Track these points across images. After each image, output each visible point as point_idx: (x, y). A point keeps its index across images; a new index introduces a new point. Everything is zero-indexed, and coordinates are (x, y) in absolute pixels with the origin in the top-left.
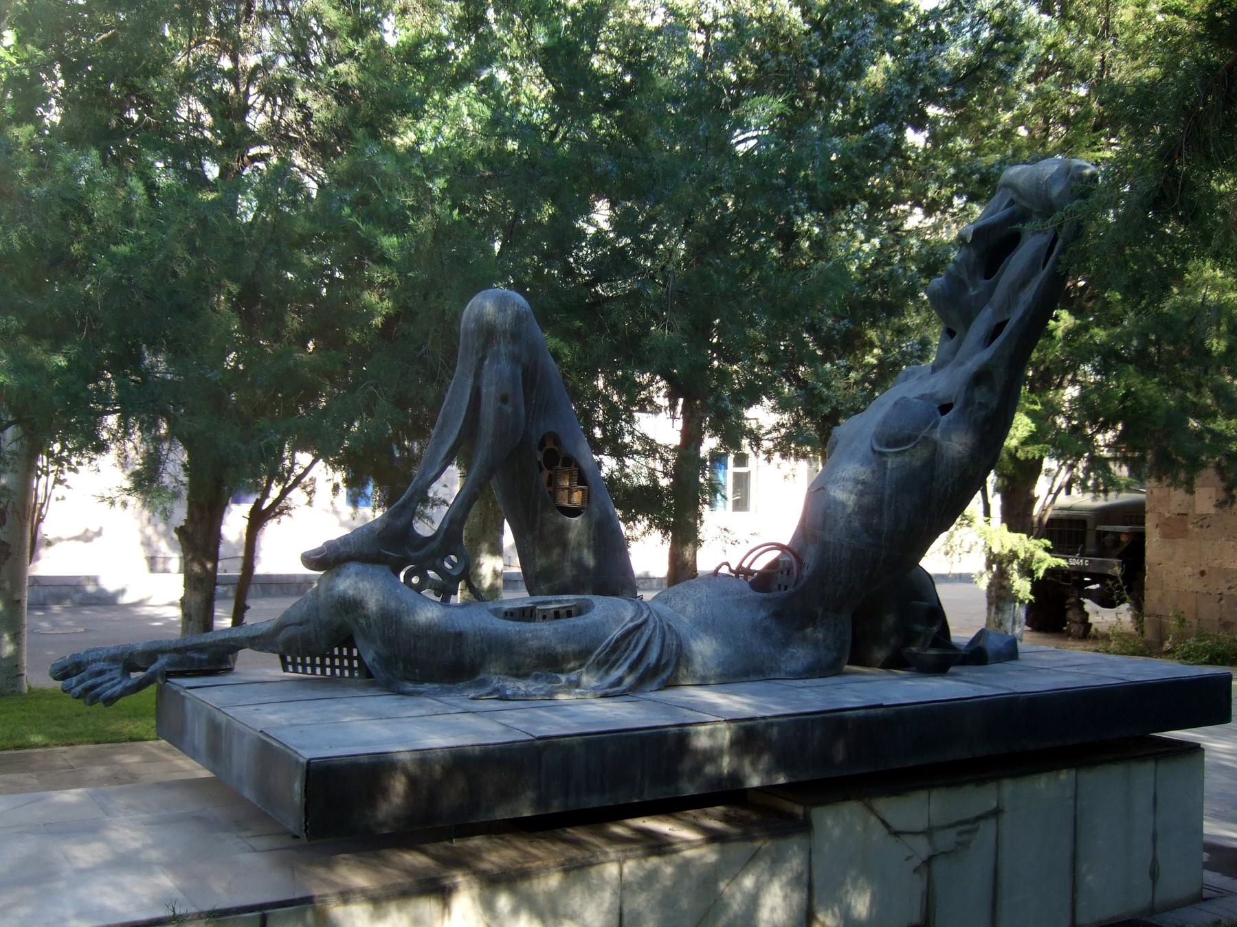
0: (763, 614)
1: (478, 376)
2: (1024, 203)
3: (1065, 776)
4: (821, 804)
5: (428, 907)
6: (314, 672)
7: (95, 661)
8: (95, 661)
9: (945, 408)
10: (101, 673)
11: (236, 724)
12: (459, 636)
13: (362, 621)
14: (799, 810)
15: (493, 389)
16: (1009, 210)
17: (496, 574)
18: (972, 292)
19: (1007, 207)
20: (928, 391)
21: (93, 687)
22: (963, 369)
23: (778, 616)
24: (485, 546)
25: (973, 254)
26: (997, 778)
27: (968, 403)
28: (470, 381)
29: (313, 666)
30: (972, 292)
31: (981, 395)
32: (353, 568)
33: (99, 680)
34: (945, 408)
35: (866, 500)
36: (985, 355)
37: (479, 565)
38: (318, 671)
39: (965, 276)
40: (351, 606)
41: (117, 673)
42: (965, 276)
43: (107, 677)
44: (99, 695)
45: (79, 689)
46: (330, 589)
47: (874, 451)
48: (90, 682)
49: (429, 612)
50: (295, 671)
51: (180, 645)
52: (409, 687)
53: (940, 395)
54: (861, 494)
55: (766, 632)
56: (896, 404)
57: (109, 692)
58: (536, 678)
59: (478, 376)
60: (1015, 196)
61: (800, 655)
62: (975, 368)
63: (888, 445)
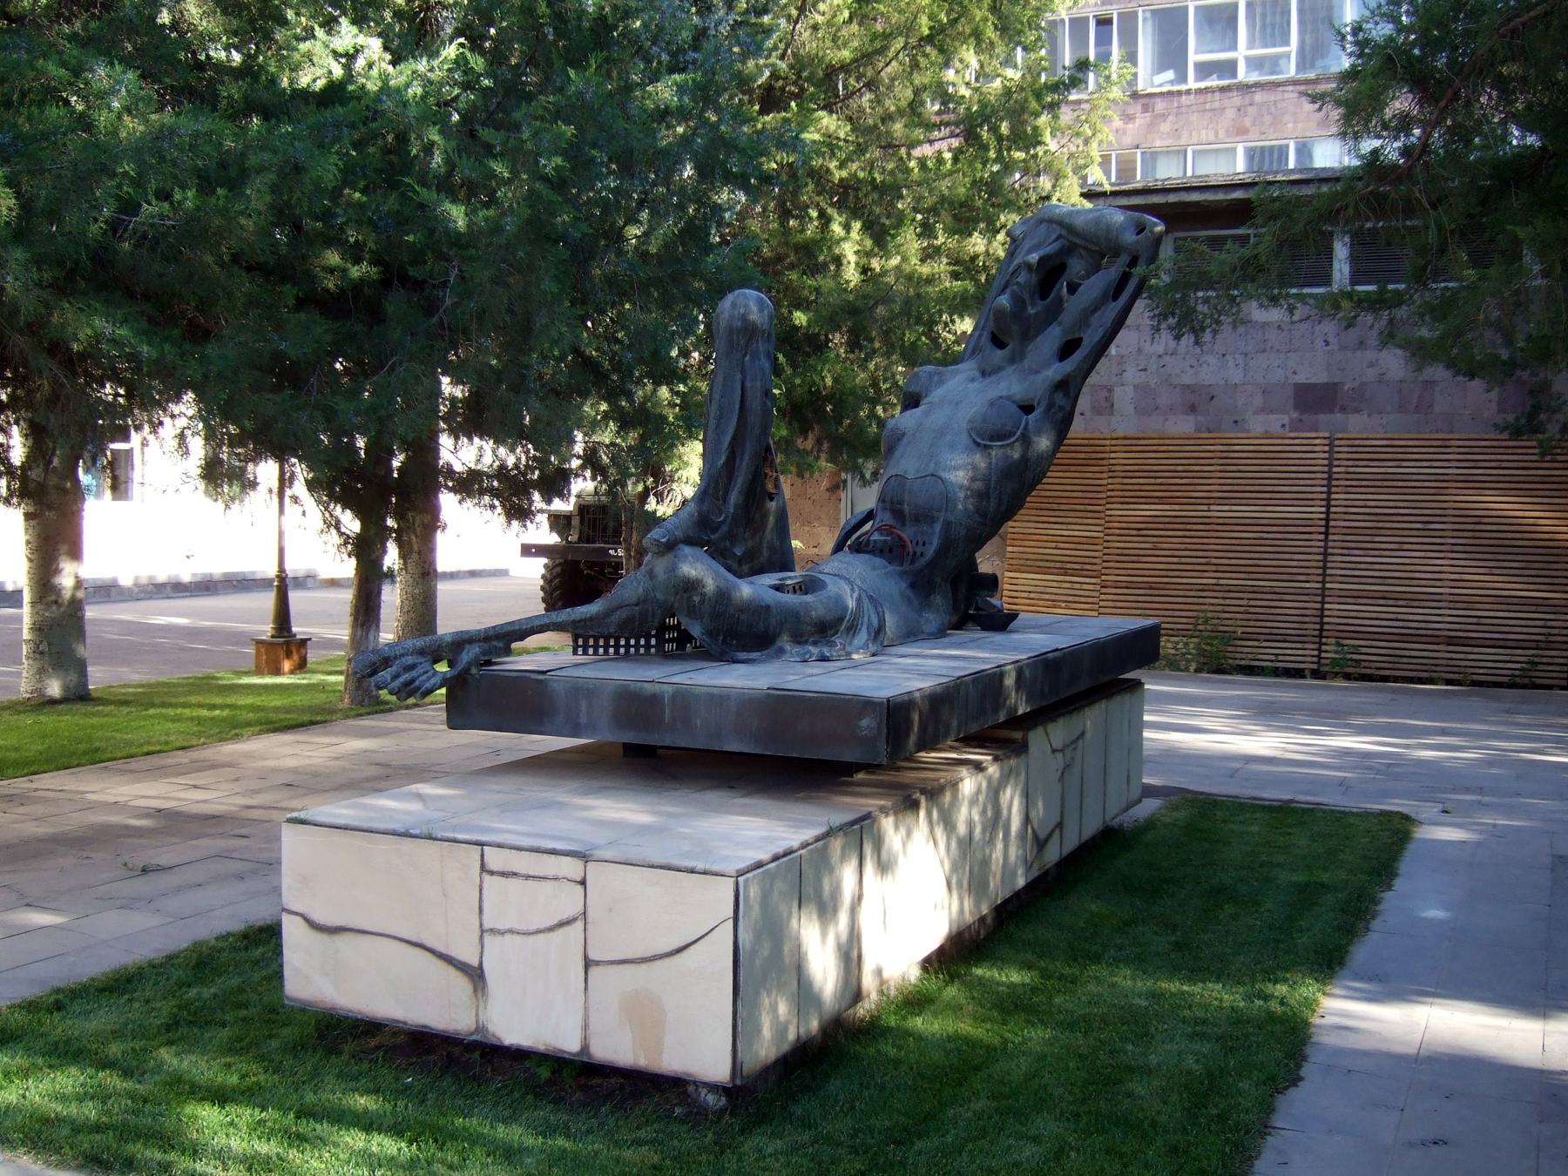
0: (904, 585)
1: (743, 372)
2: (1077, 241)
3: (1103, 704)
4: (1029, 729)
5: (909, 818)
6: (606, 652)
7: (402, 655)
8: (402, 655)
9: (1027, 409)
10: (412, 667)
11: (697, 690)
12: (768, 607)
13: (696, 599)
14: (1018, 735)
15: (758, 384)
16: (1057, 245)
17: (79, 583)
18: (1031, 311)
19: (1056, 239)
20: (1004, 393)
21: (412, 681)
22: (1040, 377)
23: (912, 586)
24: (64, 548)
25: (1034, 279)
26: (1078, 709)
27: (1051, 405)
28: (739, 376)
29: (596, 647)
30: (1031, 311)
31: (1060, 399)
32: (687, 550)
33: (414, 673)
34: (1027, 409)
35: (978, 485)
36: (1069, 366)
37: (58, 571)
38: (611, 650)
39: (1026, 297)
40: (691, 586)
41: (426, 666)
42: (1026, 297)
43: (420, 670)
44: (419, 688)
45: (397, 683)
46: (673, 569)
47: (978, 445)
48: (406, 677)
49: (746, 590)
50: (585, 653)
51: (491, 633)
52: (743, 655)
53: (1018, 397)
54: (973, 479)
55: (909, 602)
56: (992, 404)
57: (428, 685)
58: (815, 644)
59: (743, 372)
60: (1064, 233)
61: (931, 620)
62: (1058, 378)
63: (992, 439)
